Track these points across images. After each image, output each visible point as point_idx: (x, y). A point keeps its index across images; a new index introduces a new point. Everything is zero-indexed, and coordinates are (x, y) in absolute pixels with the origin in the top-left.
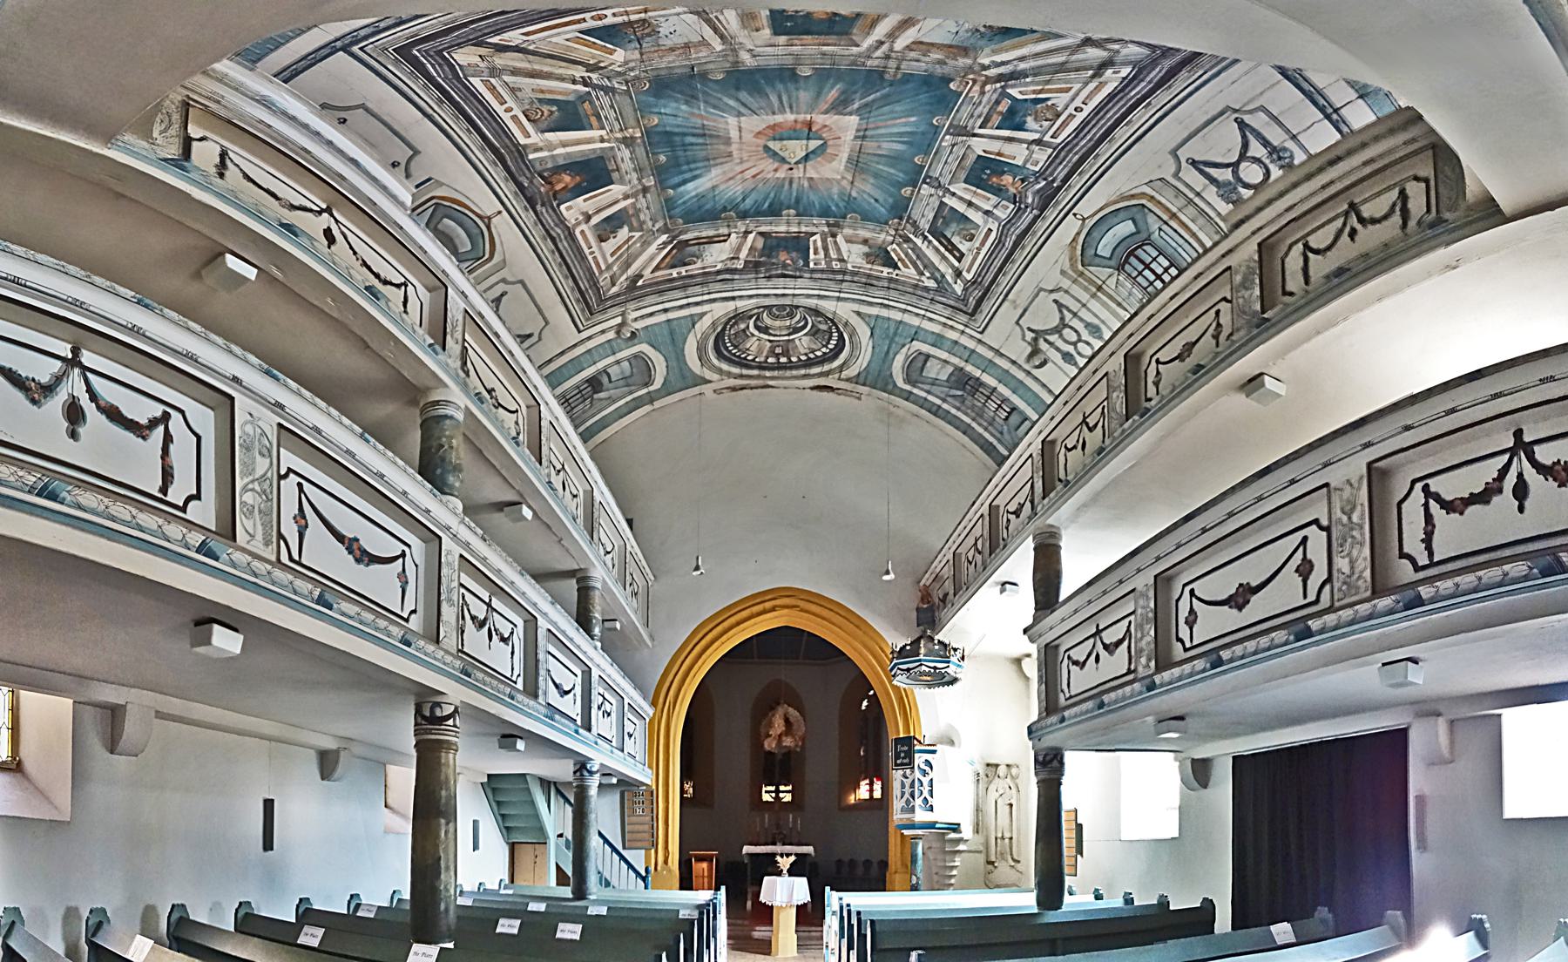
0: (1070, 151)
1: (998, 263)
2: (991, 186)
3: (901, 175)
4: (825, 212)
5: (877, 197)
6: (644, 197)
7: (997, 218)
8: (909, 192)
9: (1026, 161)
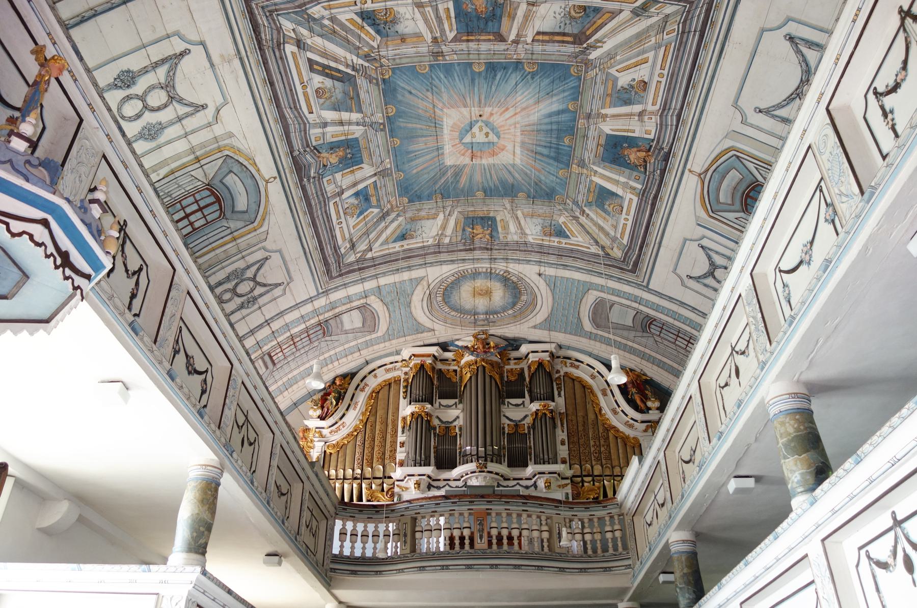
0: (320, 203)
1: (279, 86)
2: (339, 147)
3: (402, 125)
4: (448, 69)
5: (411, 97)
6: (591, 110)
7: (315, 125)
8: (390, 110)
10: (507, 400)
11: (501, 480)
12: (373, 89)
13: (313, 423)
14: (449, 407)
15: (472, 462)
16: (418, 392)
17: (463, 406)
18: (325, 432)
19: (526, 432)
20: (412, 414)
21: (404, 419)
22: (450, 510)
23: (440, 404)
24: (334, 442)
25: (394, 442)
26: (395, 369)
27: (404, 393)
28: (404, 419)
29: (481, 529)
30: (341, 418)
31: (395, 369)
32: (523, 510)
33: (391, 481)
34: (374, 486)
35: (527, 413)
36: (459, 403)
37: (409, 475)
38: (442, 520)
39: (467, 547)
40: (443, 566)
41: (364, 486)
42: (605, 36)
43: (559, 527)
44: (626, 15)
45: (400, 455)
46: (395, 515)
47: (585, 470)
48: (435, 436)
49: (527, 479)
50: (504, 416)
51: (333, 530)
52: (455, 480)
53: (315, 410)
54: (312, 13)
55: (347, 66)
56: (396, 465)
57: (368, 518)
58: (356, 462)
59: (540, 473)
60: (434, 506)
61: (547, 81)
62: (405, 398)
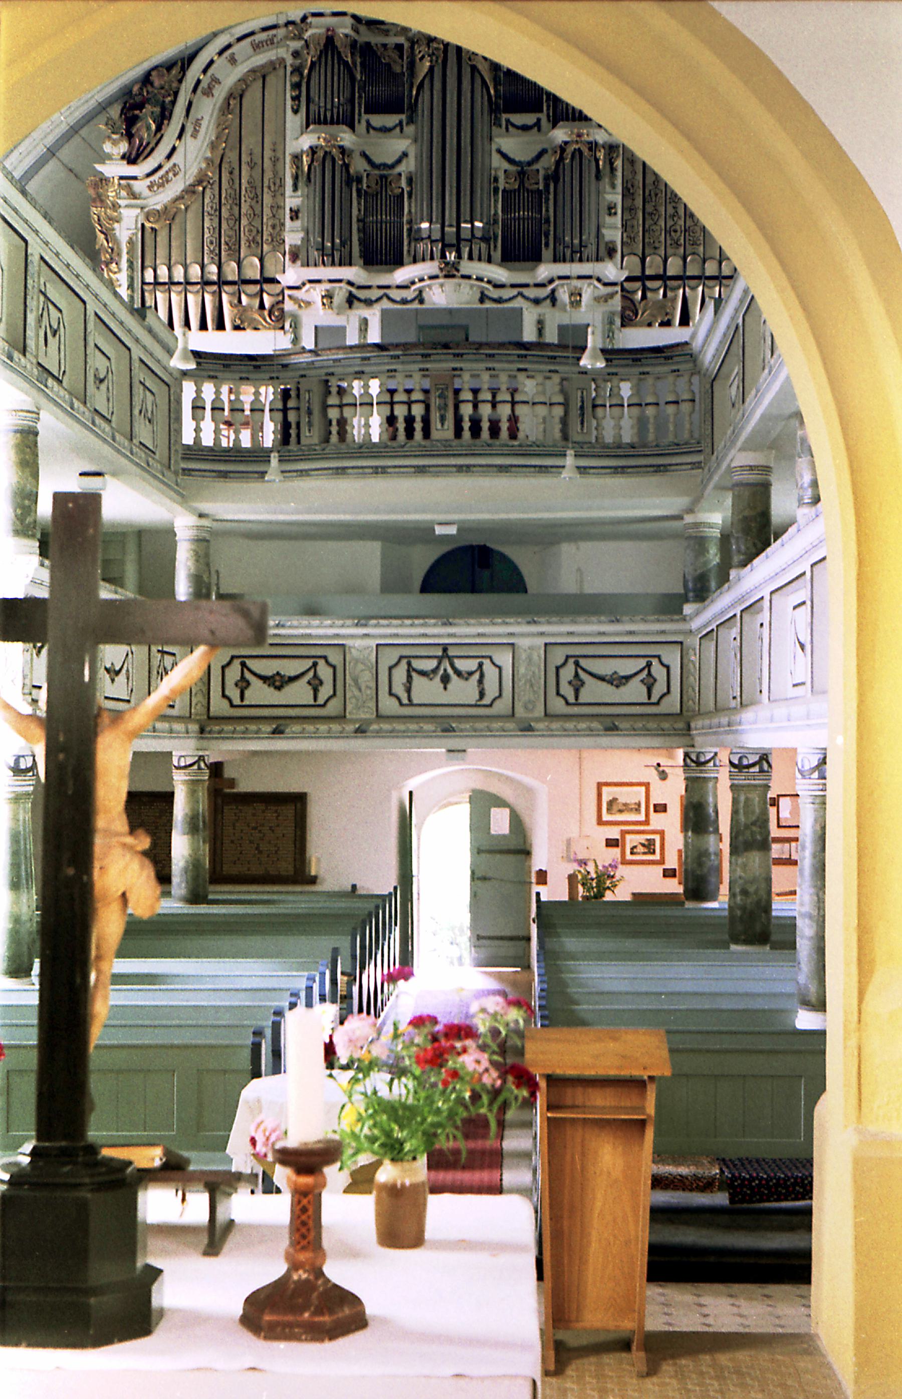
10: (504, 116)
11: (487, 289)
13: (114, 169)
14: (385, 130)
15: (432, 258)
16: (322, 99)
17: (417, 128)
18: (140, 186)
19: (541, 187)
20: (313, 150)
21: (297, 158)
22: (388, 371)
23: (369, 125)
24: (158, 207)
25: (278, 208)
26: (272, 43)
27: (293, 99)
28: (297, 158)
29: (442, 405)
30: (169, 157)
31: (272, 43)
32: (519, 370)
33: (276, 289)
34: (244, 298)
35: (545, 146)
36: (408, 124)
37: (311, 281)
38: (375, 386)
39: (418, 435)
40: (377, 467)
41: (225, 297)
43: (582, 397)
45: (293, 236)
46: (290, 374)
47: (650, 267)
48: (359, 196)
49: (537, 285)
50: (499, 151)
51: (179, 402)
52: (398, 287)
53: (115, 143)
56: (284, 255)
57: (241, 379)
58: (206, 248)
59: (560, 278)
60: (358, 361)
62: (296, 111)
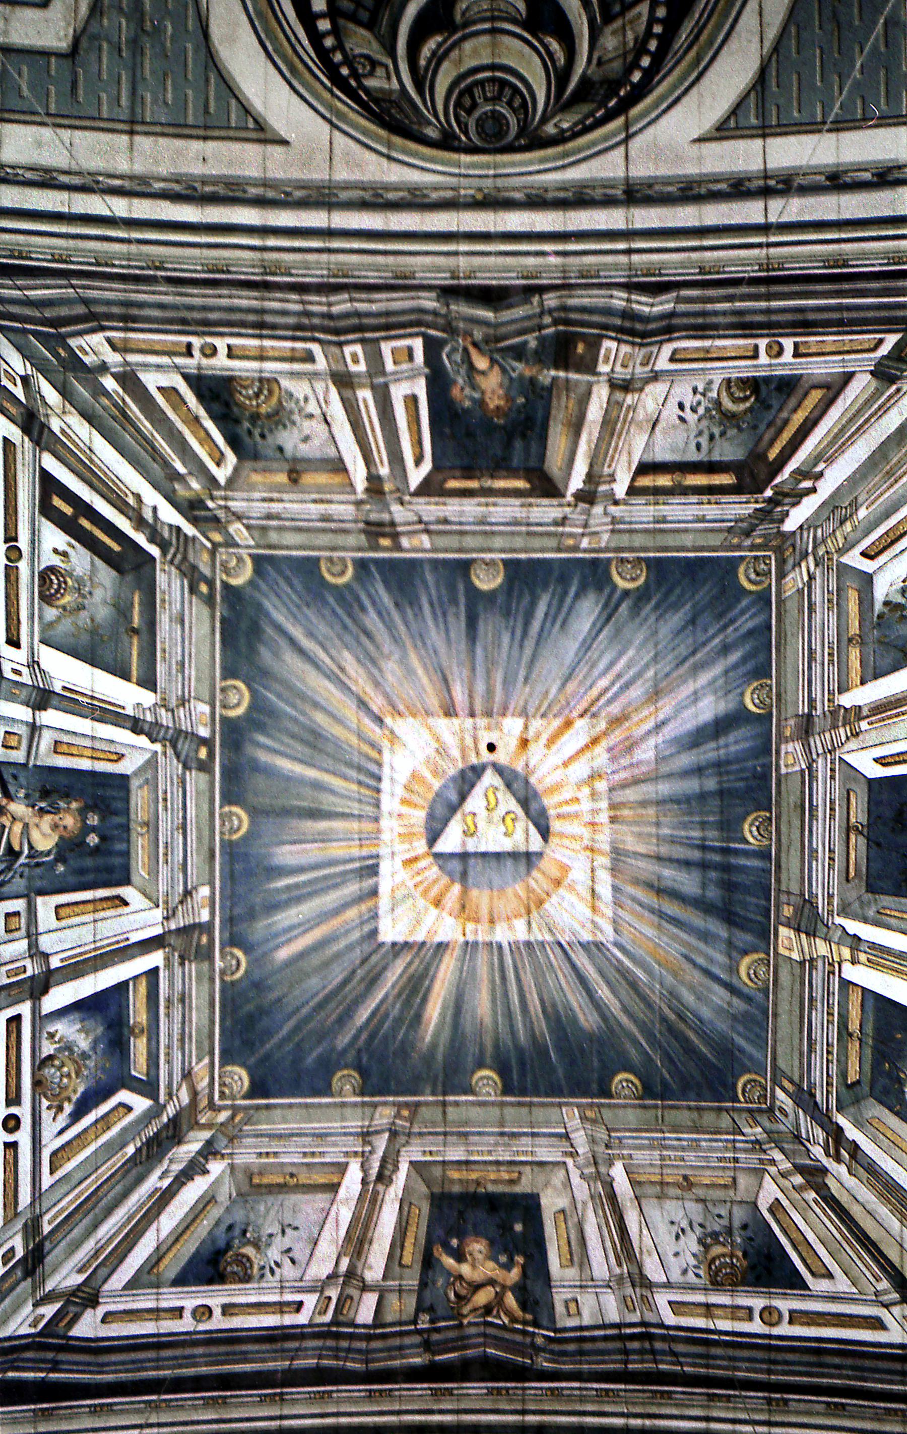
9: (32, 911)
12: (198, 613)
42: (817, 458)
44: (861, 384)
54: (81, 348)
55: (140, 523)
61: (676, 619)
